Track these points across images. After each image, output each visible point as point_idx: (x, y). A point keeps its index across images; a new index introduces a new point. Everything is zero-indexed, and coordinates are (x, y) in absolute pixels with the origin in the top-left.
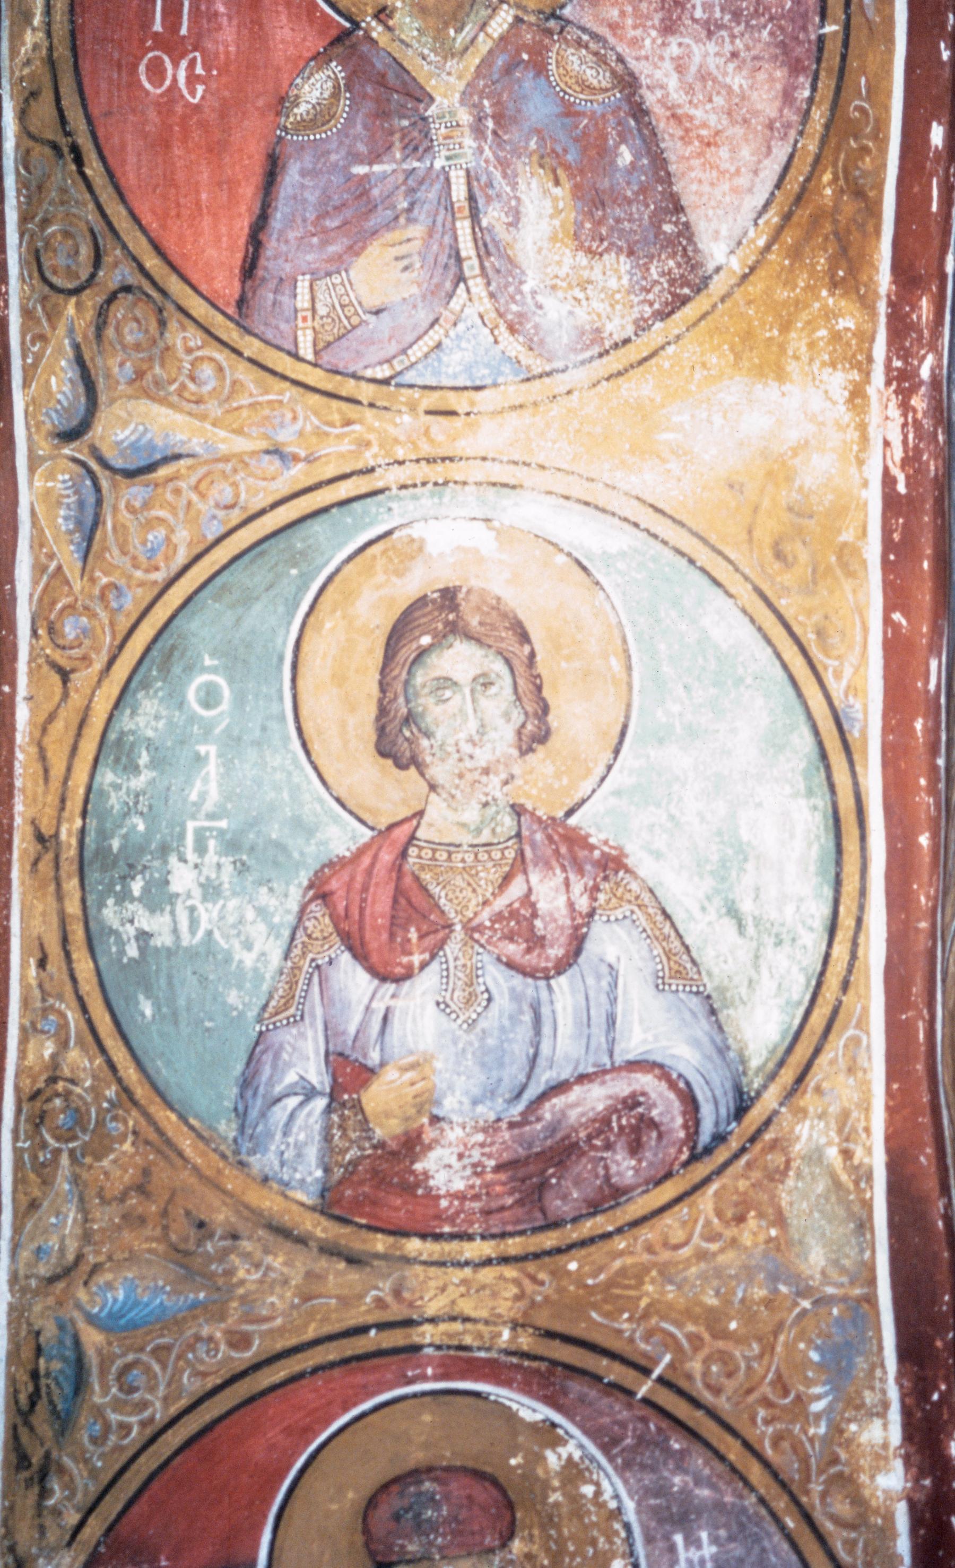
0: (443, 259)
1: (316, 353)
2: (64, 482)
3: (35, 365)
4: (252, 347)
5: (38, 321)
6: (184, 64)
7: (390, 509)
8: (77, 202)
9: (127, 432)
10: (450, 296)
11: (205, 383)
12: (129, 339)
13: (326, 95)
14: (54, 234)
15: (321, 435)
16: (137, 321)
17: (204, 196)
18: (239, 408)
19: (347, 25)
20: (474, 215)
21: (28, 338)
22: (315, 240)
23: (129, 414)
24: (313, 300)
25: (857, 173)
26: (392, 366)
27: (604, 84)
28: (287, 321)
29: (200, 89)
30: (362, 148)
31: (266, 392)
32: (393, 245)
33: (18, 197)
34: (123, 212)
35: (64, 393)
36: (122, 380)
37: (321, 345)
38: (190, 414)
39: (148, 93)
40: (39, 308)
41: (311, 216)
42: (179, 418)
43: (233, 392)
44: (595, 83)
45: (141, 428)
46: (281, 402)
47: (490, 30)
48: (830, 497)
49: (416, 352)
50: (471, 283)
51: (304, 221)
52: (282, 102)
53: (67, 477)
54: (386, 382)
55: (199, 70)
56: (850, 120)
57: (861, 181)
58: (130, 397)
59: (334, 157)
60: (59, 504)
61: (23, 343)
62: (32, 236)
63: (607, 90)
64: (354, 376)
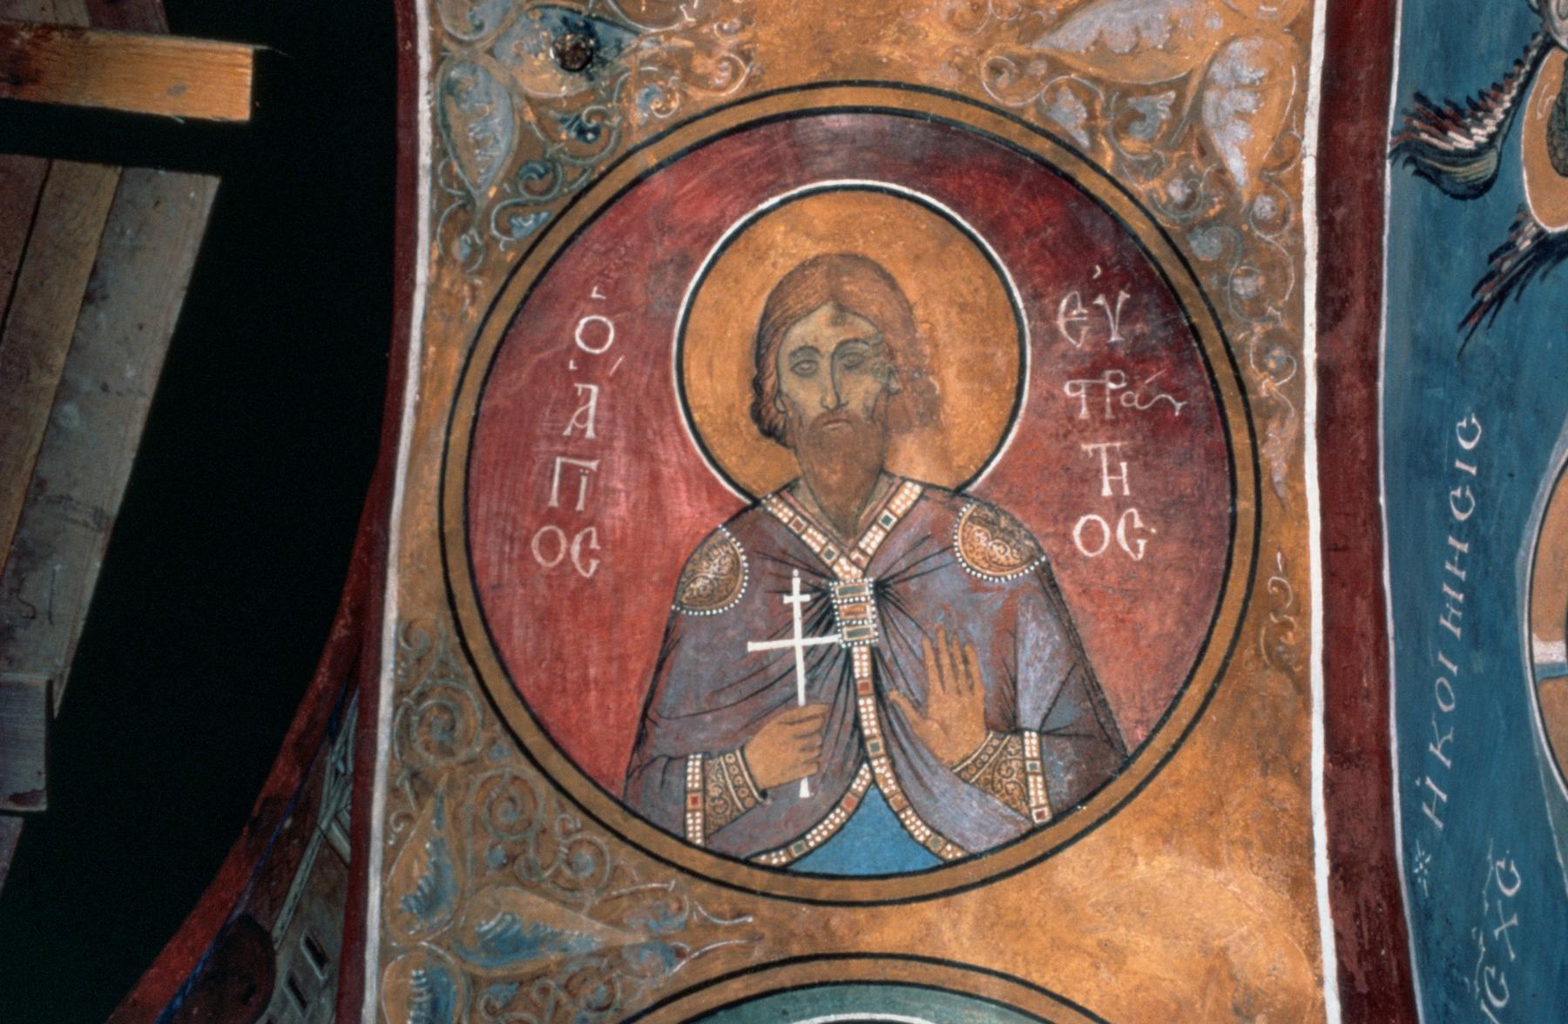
0: (845, 737)
1: (706, 837)
2: (418, 978)
3: (397, 848)
4: (635, 830)
5: (405, 801)
6: (578, 538)
7: (785, 1013)
8: (457, 675)
9: (492, 923)
10: (855, 775)
11: (583, 869)
12: (502, 820)
13: (725, 570)
14: (430, 708)
15: (708, 927)
16: (512, 800)
17: (592, 671)
18: (620, 896)
19: (748, 502)
20: (879, 695)
21: (392, 817)
22: (709, 718)
23: (497, 903)
24: (704, 780)
25: (1281, 648)
26: (789, 853)
27: (1012, 561)
28: (676, 802)
29: (594, 564)
30: (760, 624)
31: (652, 881)
32: (792, 723)
33: (395, 670)
34: (505, 685)
35: (426, 879)
36: (492, 865)
37: (712, 829)
38: (564, 903)
39: (539, 566)
40: (407, 786)
41: (704, 691)
42: (552, 906)
43: (612, 878)
44: (1003, 558)
45: (508, 918)
46: (664, 890)
47: (893, 507)
48: (1282, 996)
49: (814, 838)
50: (875, 763)
51: (698, 697)
52: (678, 576)
53: (421, 972)
54: (782, 869)
55: (594, 545)
56: (1267, 595)
57: (1286, 657)
58: (499, 884)
59: (731, 633)
60: (410, 1004)
61: (386, 823)
62: (407, 710)
63: (1014, 566)
64: (747, 862)
